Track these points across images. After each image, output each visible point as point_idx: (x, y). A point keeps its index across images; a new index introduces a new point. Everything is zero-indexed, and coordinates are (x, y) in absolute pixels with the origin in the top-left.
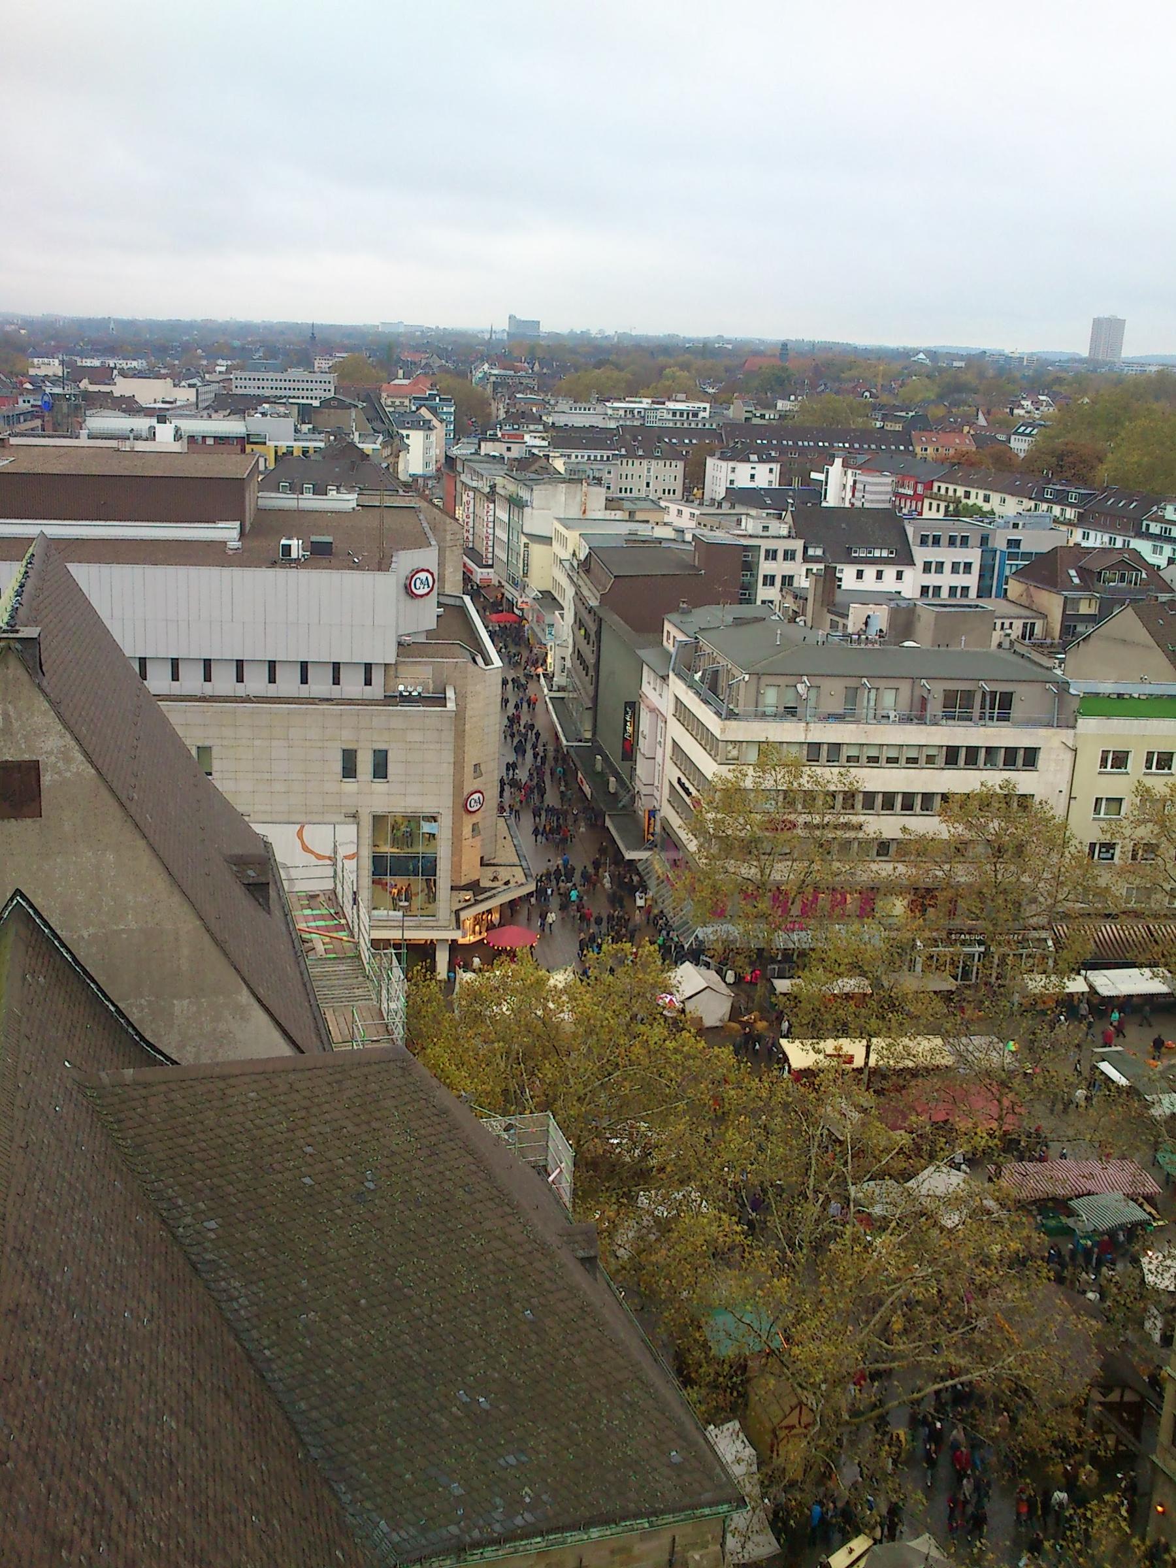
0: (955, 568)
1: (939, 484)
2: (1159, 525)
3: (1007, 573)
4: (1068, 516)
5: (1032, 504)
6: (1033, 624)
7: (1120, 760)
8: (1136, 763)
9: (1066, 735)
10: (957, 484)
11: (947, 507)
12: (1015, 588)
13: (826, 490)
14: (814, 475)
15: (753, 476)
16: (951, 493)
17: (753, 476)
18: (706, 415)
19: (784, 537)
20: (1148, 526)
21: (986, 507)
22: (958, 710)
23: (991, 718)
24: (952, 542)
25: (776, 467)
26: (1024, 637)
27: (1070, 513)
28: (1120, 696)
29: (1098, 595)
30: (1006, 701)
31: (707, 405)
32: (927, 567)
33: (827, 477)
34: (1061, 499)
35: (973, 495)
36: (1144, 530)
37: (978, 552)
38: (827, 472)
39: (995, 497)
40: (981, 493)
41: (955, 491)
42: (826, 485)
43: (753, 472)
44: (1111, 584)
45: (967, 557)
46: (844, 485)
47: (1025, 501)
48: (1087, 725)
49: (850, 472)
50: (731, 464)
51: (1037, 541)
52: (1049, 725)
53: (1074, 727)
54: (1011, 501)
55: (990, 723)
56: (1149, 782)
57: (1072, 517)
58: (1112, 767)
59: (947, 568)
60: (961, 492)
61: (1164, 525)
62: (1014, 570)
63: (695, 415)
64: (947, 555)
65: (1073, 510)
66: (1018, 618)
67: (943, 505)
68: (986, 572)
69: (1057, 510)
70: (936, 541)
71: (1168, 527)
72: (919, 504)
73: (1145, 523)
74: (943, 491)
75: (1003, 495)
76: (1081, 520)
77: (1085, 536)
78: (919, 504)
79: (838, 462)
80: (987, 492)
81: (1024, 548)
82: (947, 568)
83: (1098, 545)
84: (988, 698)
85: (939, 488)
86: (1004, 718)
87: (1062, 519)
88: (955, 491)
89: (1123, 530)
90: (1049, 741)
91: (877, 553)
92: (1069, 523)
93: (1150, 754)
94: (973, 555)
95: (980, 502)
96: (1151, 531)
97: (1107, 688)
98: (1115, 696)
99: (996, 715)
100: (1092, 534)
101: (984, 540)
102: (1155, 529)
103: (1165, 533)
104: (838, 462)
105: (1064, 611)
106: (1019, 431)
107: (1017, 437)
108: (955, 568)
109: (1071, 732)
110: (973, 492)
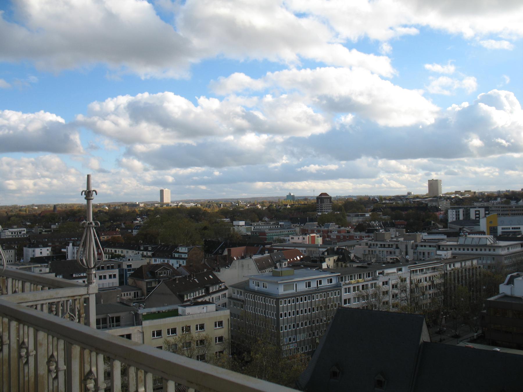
0: (110, 276)
1: (106, 249)
2: (178, 254)
3: (128, 276)
4: (149, 255)
5: (137, 252)
6: (137, 293)
7: (159, 333)
8: (164, 333)
9: (139, 328)
10: (112, 248)
11: (109, 256)
12: (130, 281)
13: (67, 255)
14: (63, 250)
15: (41, 253)
16: (110, 251)
17: (41, 253)
18: (25, 232)
19: (48, 273)
20: (174, 255)
21: (122, 254)
22: (101, 325)
23: (113, 326)
24: (108, 268)
25: (50, 249)
26: (135, 297)
27: (150, 254)
28: (159, 312)
29: (157, 280)
30: (118, 319)
31: (25, 229)
32: (100, 278)
33: (67, 250)
34: (146, 249)
35: (117, 251)
36: (173, 256)
37: (117, 270)
38: (67, 249)
39: (125, 251)
40: (120, 250)
41: (111, 250)
42: (67, 253)
43: (41, 251)
44: (161, 275)
45: (113, 273)
46: (74, 253)
47: (135, 251)
48: (146, 323)
49: (75, 248)
50: (32, 249)
51: (136, 264)
52: (133, 325)
53: (142, 324)
54: (130, 252)
55: (112, 328)
56: (168, 339)
57: (150, 255)
58: (156, 336)
59: (108, 277)
60: (113, 250)
61: (179, 254)
62: (130, 274)
63: (20, 233)
64: (107, 273)
65: (150, 252)
66: (132, 290)
67: (108, 256)
68: (121, 276)
69: (145, 253)
70: (103, 268)
71: (181, 254)
72: (100, 256)
73: (173, 254)
74: (107, 251)
75: (128, 250)
76: (154, 256)
77: (155, 261)
78: (100, 256)
79: (71, 244)
80: (122, 250)
81: (133, 267)
82: (108, 277)
83: (159, 263)
84: (111, 319)
85: (106, 250)
86: (118, 326)
87: (147, 256)
88: (111, 250)
89: (167, 257)
90: (133, 330)
91: (82, 275)
92: (149, 257)
93: (168, 330)
94: (116, 272)
95: (120, 253)
96: (175, 256)
97: (154, 310)
98: (157, 312)
99: (115, 324)
100: (157, 259)
101: (119, 266)
102: (177, 255)
103: (180, 256)
104: (71, 244)
105: (147, 287)
106: (135, 228)
107: (135, 230)
108: (110, 276)
109: (140, 326)
110: (117, 250)
